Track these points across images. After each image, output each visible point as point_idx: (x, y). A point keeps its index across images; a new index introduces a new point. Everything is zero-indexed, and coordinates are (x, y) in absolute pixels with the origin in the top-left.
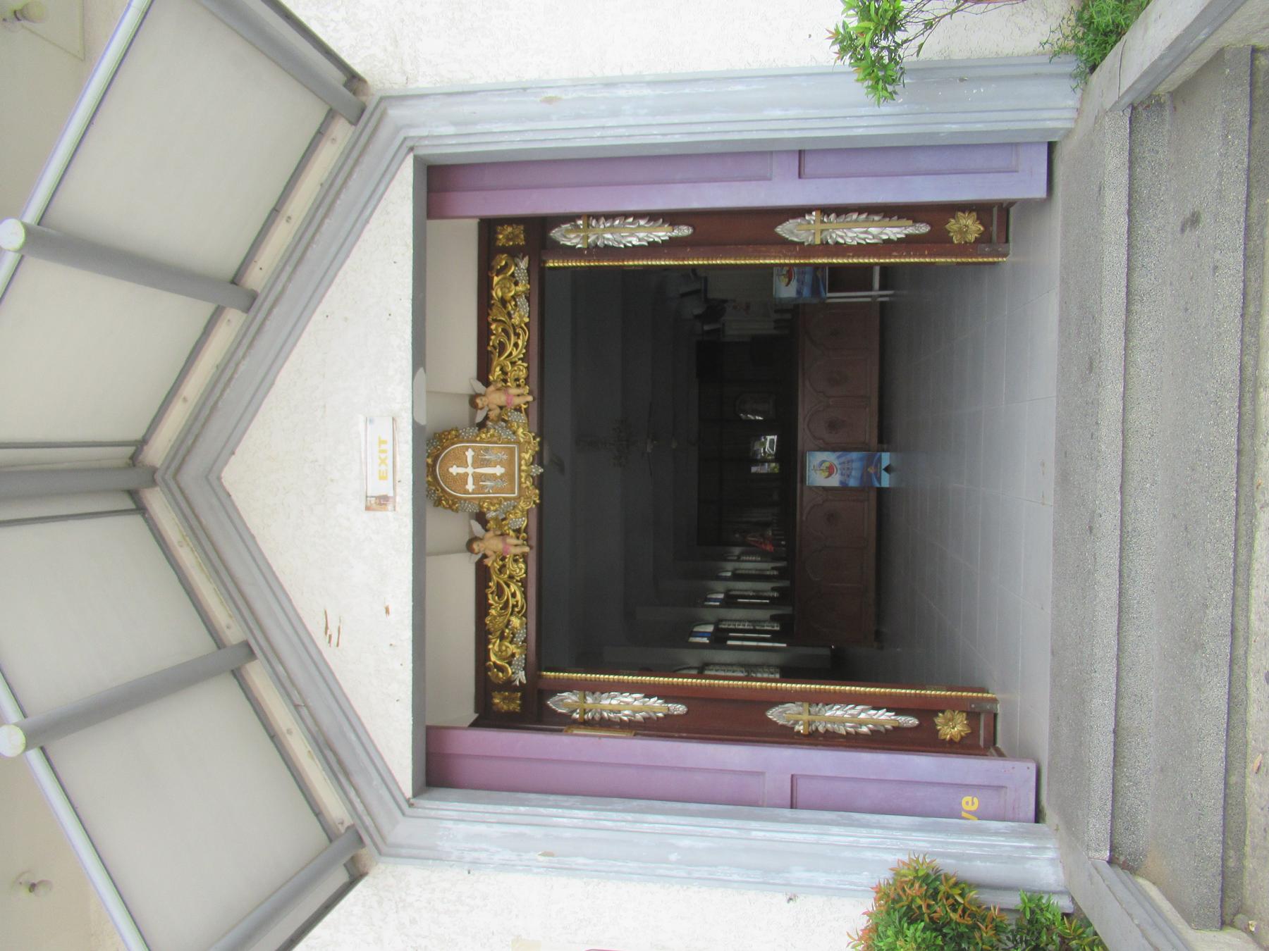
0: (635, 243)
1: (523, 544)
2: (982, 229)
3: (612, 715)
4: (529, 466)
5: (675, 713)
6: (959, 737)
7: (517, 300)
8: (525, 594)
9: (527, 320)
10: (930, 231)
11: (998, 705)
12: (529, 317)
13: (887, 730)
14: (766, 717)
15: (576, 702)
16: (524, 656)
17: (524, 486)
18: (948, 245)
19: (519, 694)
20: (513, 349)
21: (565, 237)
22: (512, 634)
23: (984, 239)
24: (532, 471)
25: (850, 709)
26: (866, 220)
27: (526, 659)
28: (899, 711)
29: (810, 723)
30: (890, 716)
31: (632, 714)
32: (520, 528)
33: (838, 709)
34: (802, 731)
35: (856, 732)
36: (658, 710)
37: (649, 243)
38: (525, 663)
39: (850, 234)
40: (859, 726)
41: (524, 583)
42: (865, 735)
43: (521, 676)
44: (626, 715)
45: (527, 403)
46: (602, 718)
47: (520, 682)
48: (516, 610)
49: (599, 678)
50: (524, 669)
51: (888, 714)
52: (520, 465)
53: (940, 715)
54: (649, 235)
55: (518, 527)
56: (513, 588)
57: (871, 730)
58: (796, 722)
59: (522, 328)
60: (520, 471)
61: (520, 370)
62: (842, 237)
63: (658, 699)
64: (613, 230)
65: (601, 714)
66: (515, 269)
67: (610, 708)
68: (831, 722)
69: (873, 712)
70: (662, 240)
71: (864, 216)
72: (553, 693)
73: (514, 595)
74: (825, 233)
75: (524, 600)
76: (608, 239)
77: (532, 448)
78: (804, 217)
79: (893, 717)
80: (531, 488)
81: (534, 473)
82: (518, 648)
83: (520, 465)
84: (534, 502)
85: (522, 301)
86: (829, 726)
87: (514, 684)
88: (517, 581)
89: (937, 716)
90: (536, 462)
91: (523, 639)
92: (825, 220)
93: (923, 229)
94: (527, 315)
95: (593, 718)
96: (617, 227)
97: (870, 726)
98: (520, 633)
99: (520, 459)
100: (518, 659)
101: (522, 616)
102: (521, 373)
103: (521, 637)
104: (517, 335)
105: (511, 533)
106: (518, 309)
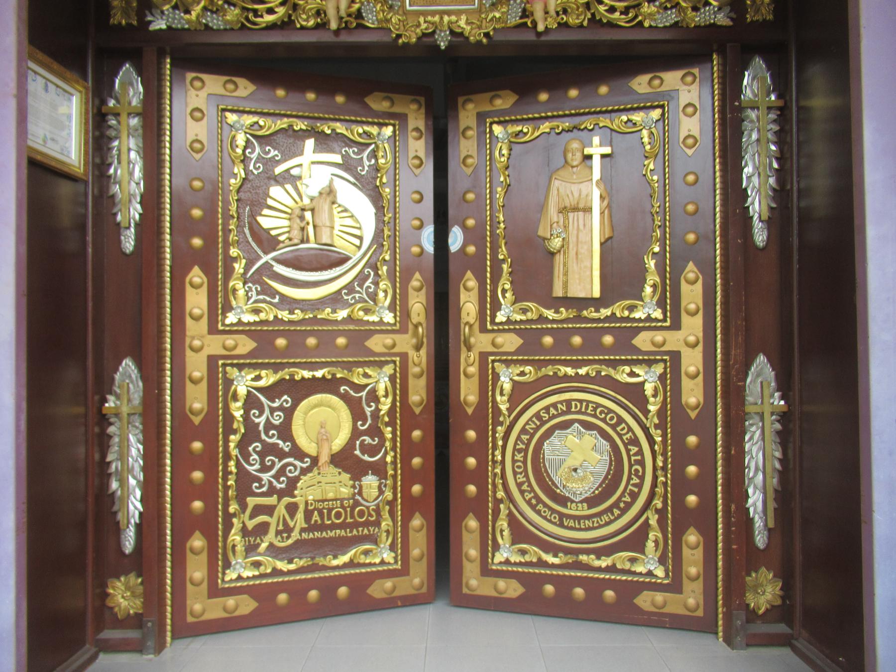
0: (746, 170)
1: (341, 18)
2: (761, 612)
3: (115, 152)
4: (449, 27)
5: (123, 238)
6: (111, 605)
7: (674, 10)
8: (272, 27)
9: (646, 24)
10: (757, 548)
11: (151, 656)
12: (651, 26)
13: (116, 513)
14: (125, 357)
15: (130, 103)
16: (187, 26)
17: (422, 20)
18: (743, 573)
19: (135, 23)
20: (606, 5)
21: (753, 79)
22: (217, 10)
23: (752, 615)
24: (441, 31)
25: (140, 464)
26: (774, 469)
27: (183, 29)
28: (139, 527)
29: (117, 415)
30: (134, 516)
31: (117, 180)
32: (363, 18)
33: (139, 450)
34: (107, 405)
35: (110, 475)
36: (123, 214)
37: (745, 189)
38: (177, 30)
39: (754, 449)
40: (118, 477)
41: (286, 24)
42: (108, 485)
43: (160, 24)
44: (116, 171)
45: (535, 24)
46: (111, 139)
47: (150, 22)
48: (251, 15)
49: (165, 134)
50: (169, 28)
51: (137, 513)
52: (449, 13)
53: (140, 580)
54: (755, 190)
55: (364, 14)
56: (281, 11)
57: (114, 493)
58: (118, 397)
59: (636, 17)
60: (442, 13)
61: (578, 16)
62: (751, 438)
63: (140, 214)
64: (763, 141)
65: (116, 138)
66: (714, 7)
67: (124, 149)
68: (121, 441)
69: (138, 493)
70: (748, 207)
71: (778, 465)
72: (140, 73)
73: (271, 11)
74: (757, 418)
75: (264, 25)
76: (750, 136)
77: (474, 32)
78: (778, 390)
79: (133, 521)
80: (418, 31)
81: (440, 35)
82: (198, 17)
83: (449, 13)
84: (399, 36)
85: (672, 17)
86: (117, 440)
87: (147, 12)
88: (290, 16)
89: (139, 576)
90: (454, 39)
91: (210, 24)
92: (774, 417)
93: (760, 540)
94: (653, 24)
95: (110, 127)
96: (768, 149)
97: (119, 492)
98: (218, 20)
99: (458, 13)
100: (182, 18)
101: (243, 24)
102: (575, 17)
103: (212, 21)
104: (625, 12)
105: (357, 6)
106: (661, 11)
